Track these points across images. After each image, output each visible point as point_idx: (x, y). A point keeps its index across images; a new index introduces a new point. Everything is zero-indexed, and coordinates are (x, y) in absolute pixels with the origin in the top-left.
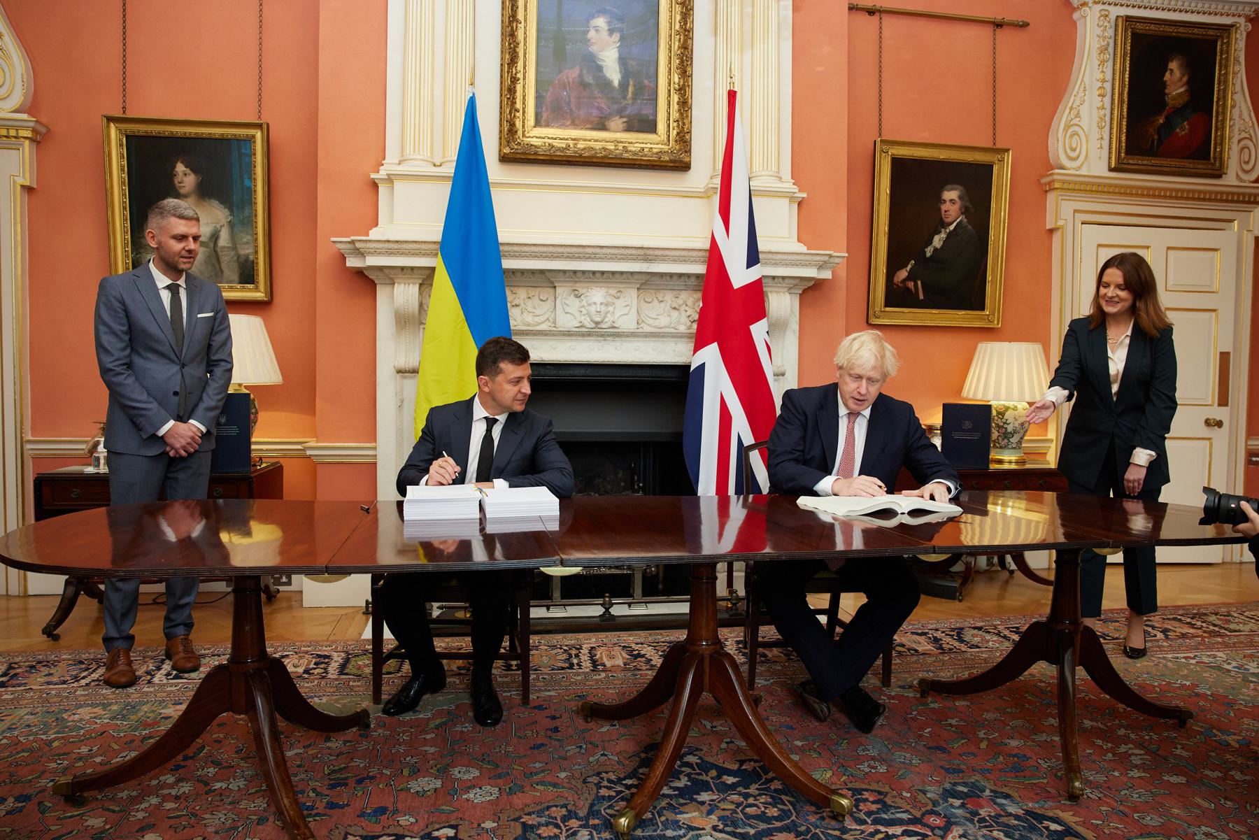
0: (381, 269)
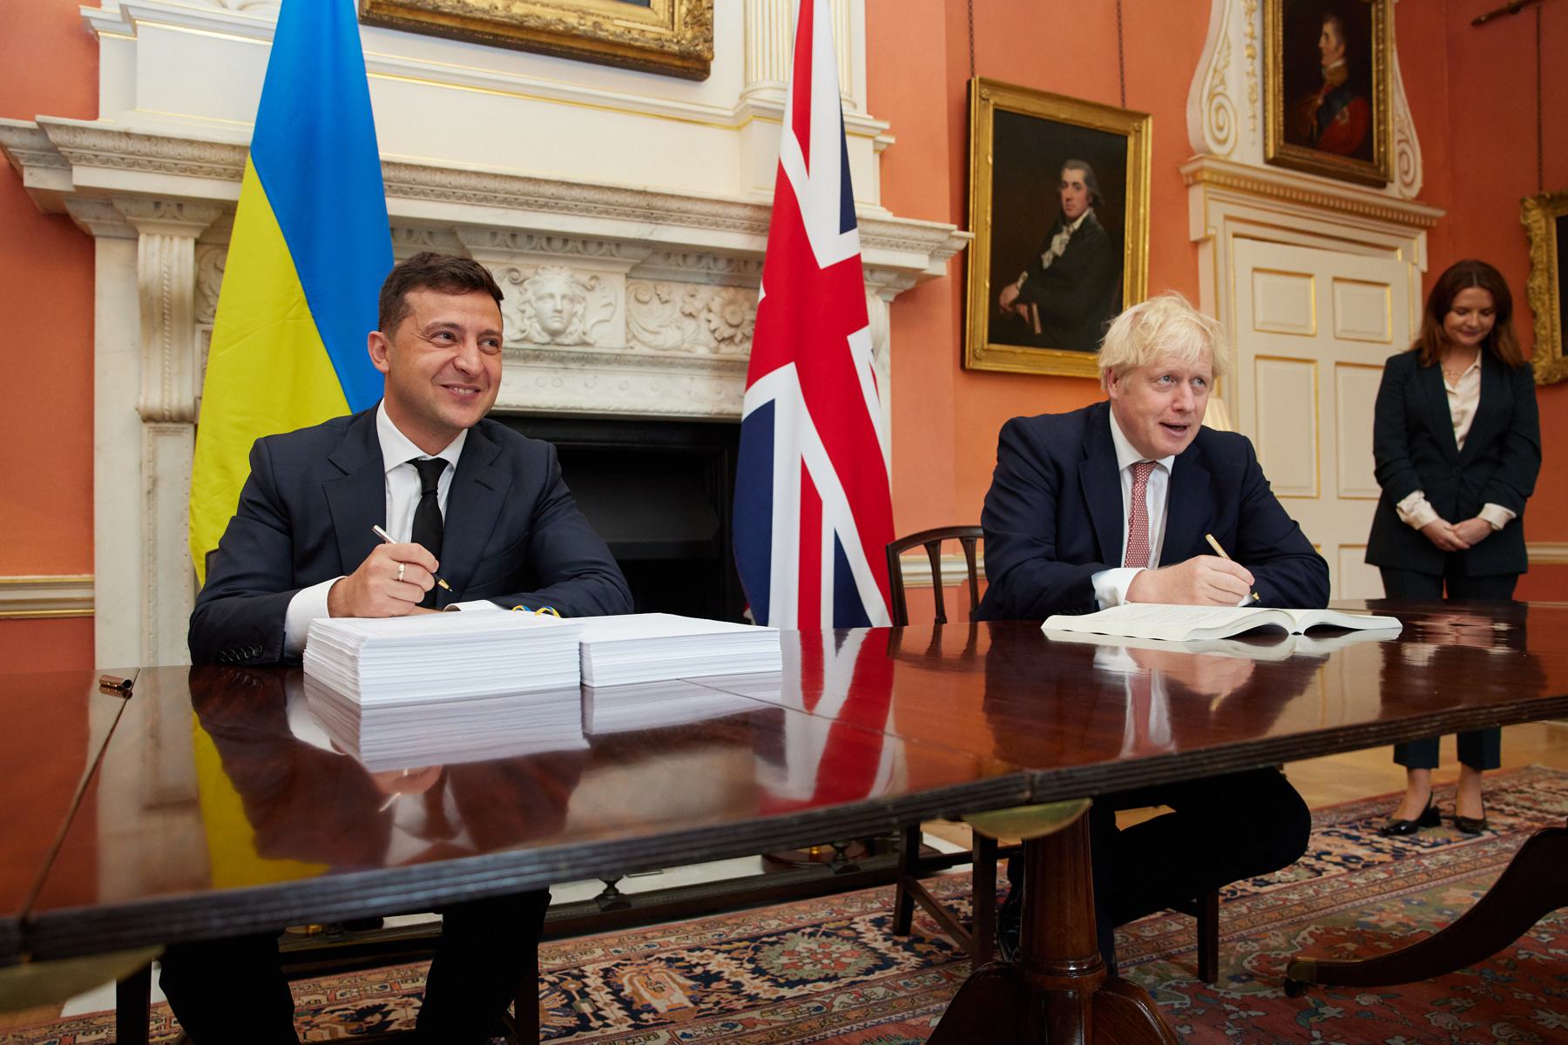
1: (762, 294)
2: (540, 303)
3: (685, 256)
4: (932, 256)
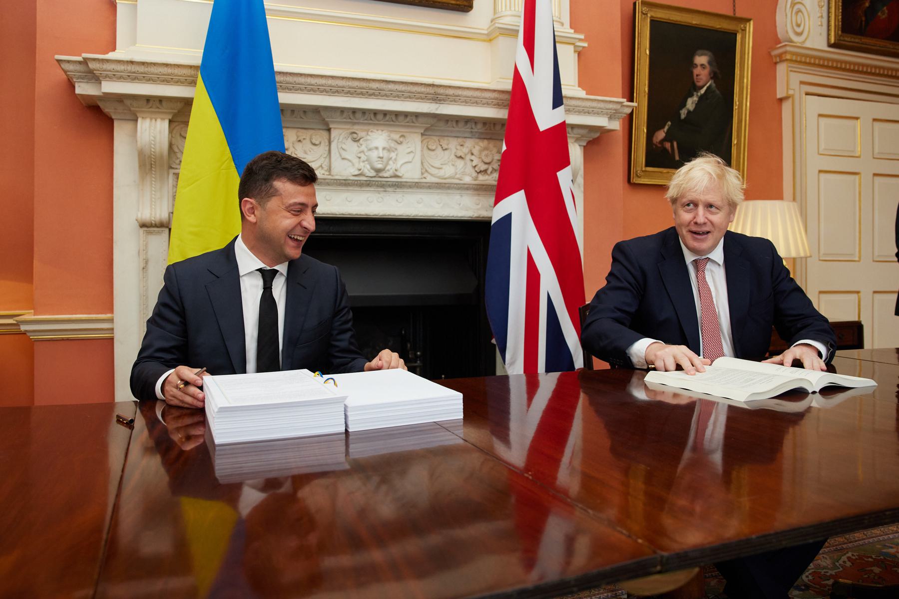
0: (120, 99)
1: (504, 148)
2: (370, 153)
3: (457, 122)
4: (611, 118)
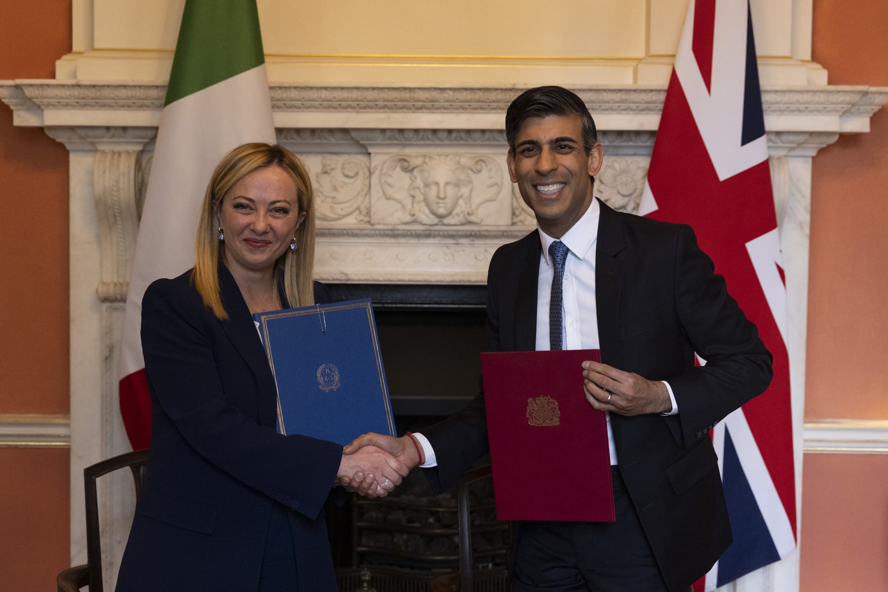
0: (72, 128)
